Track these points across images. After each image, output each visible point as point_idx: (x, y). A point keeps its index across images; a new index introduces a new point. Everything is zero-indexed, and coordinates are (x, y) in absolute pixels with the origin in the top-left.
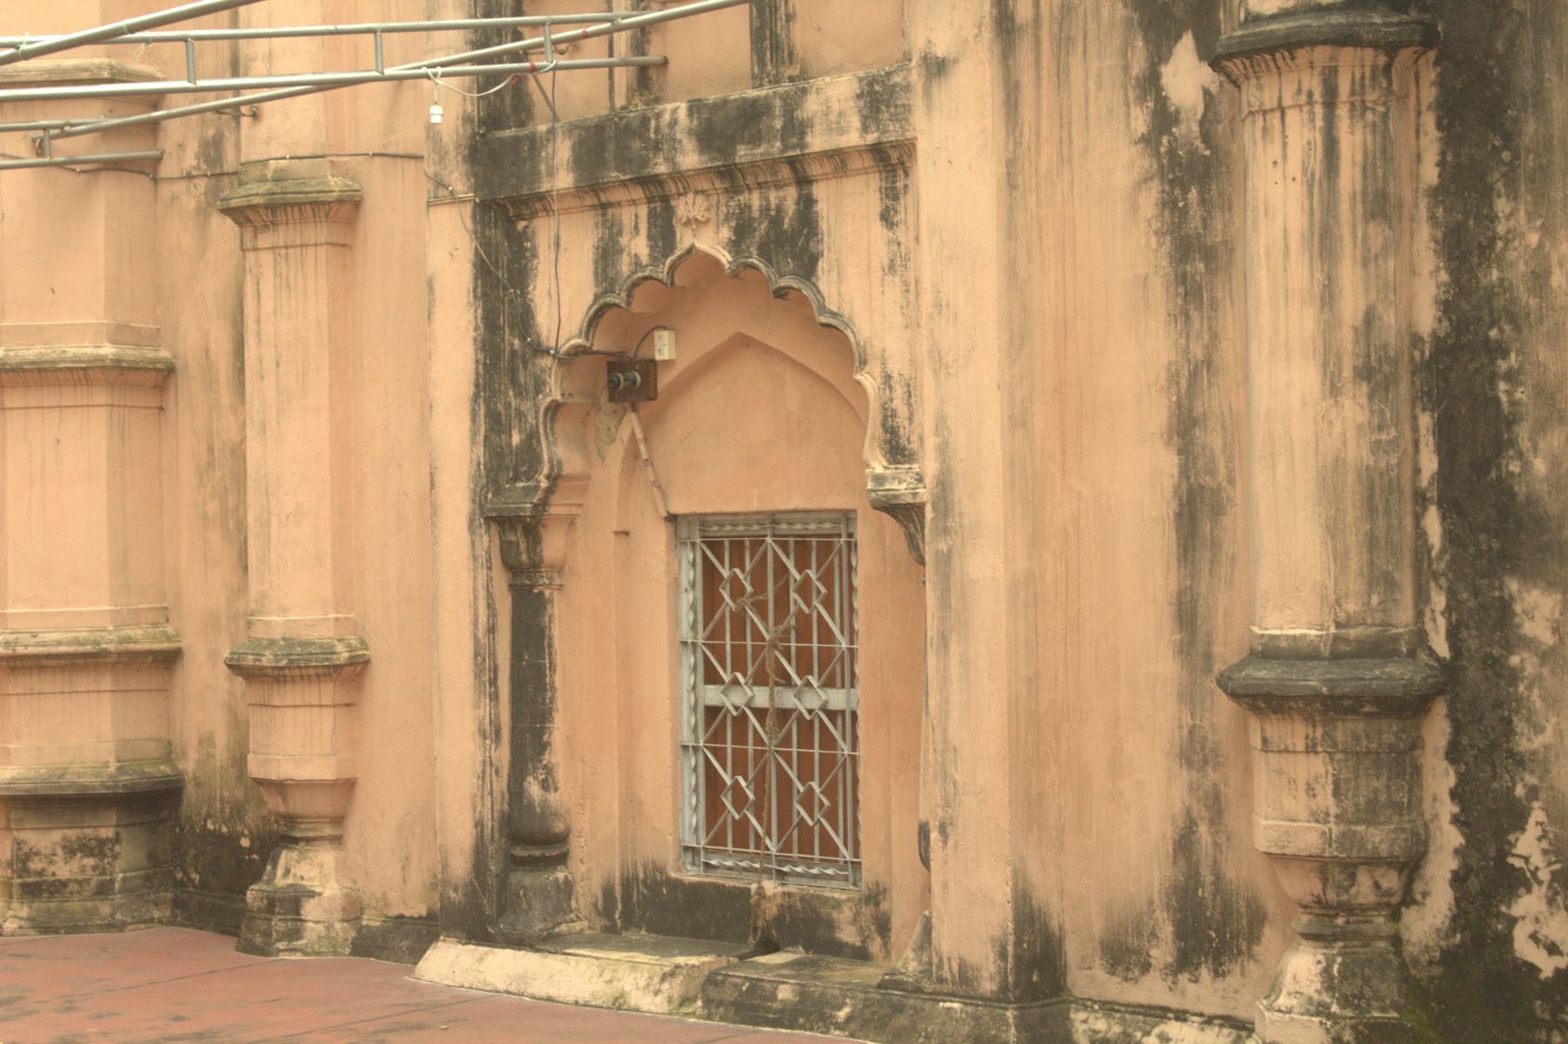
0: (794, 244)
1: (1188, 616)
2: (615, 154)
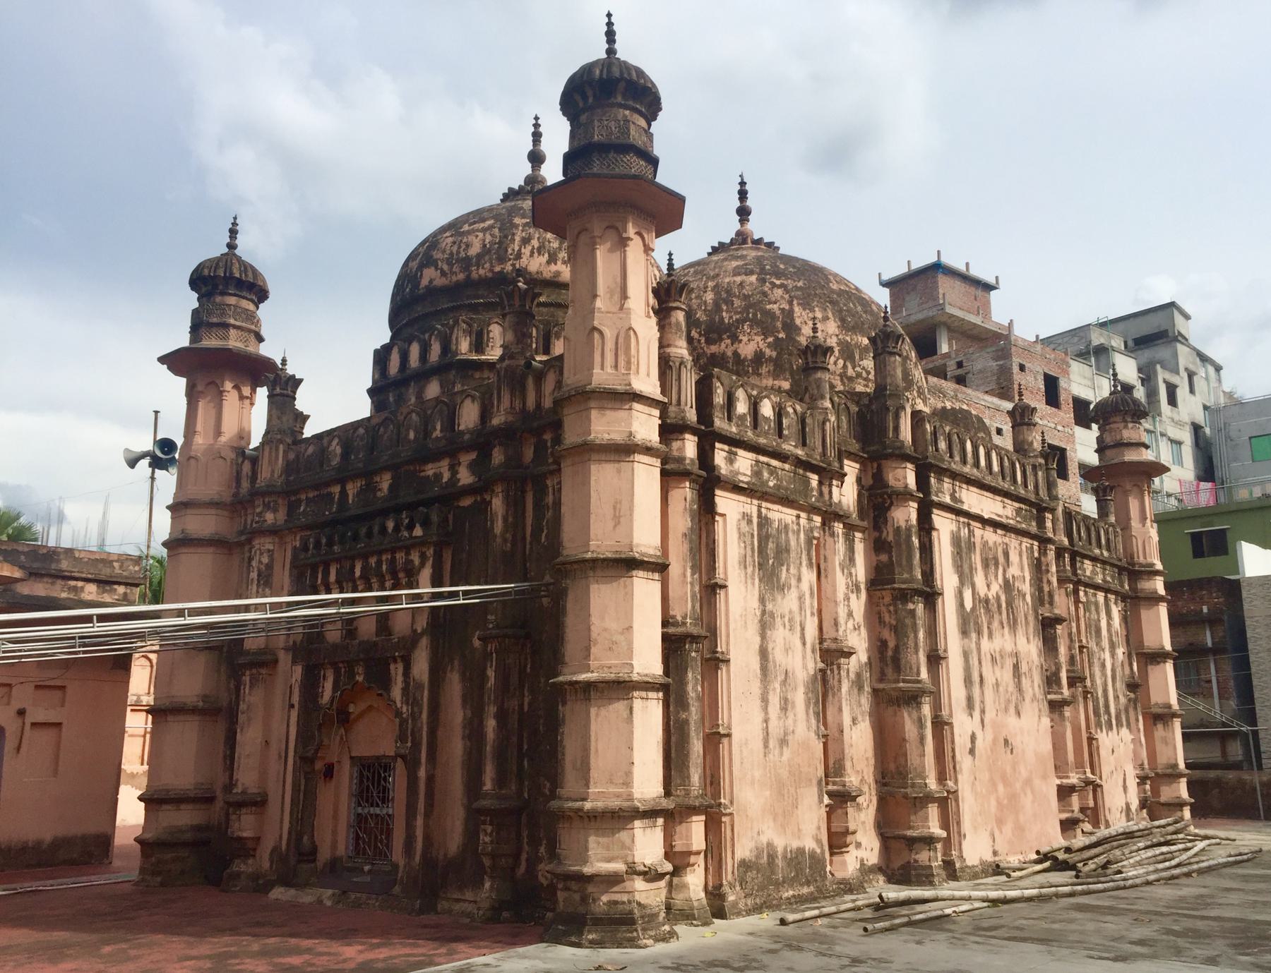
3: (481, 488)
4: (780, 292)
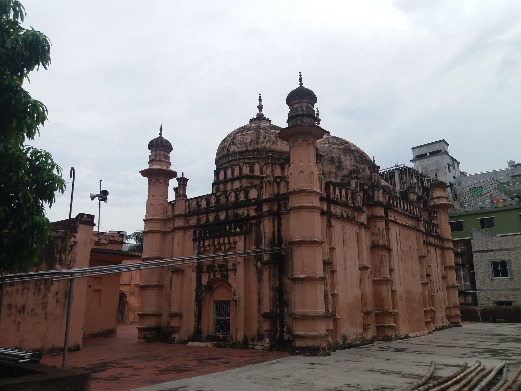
0: (227, 277)
1: (259, 310)
2: (211, 268)
3: (260, 217)
4: (336, 150)
